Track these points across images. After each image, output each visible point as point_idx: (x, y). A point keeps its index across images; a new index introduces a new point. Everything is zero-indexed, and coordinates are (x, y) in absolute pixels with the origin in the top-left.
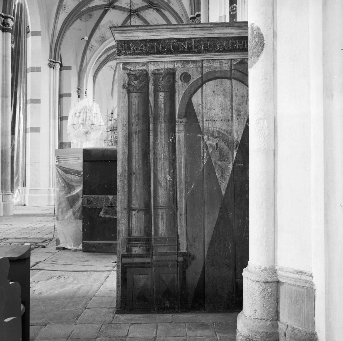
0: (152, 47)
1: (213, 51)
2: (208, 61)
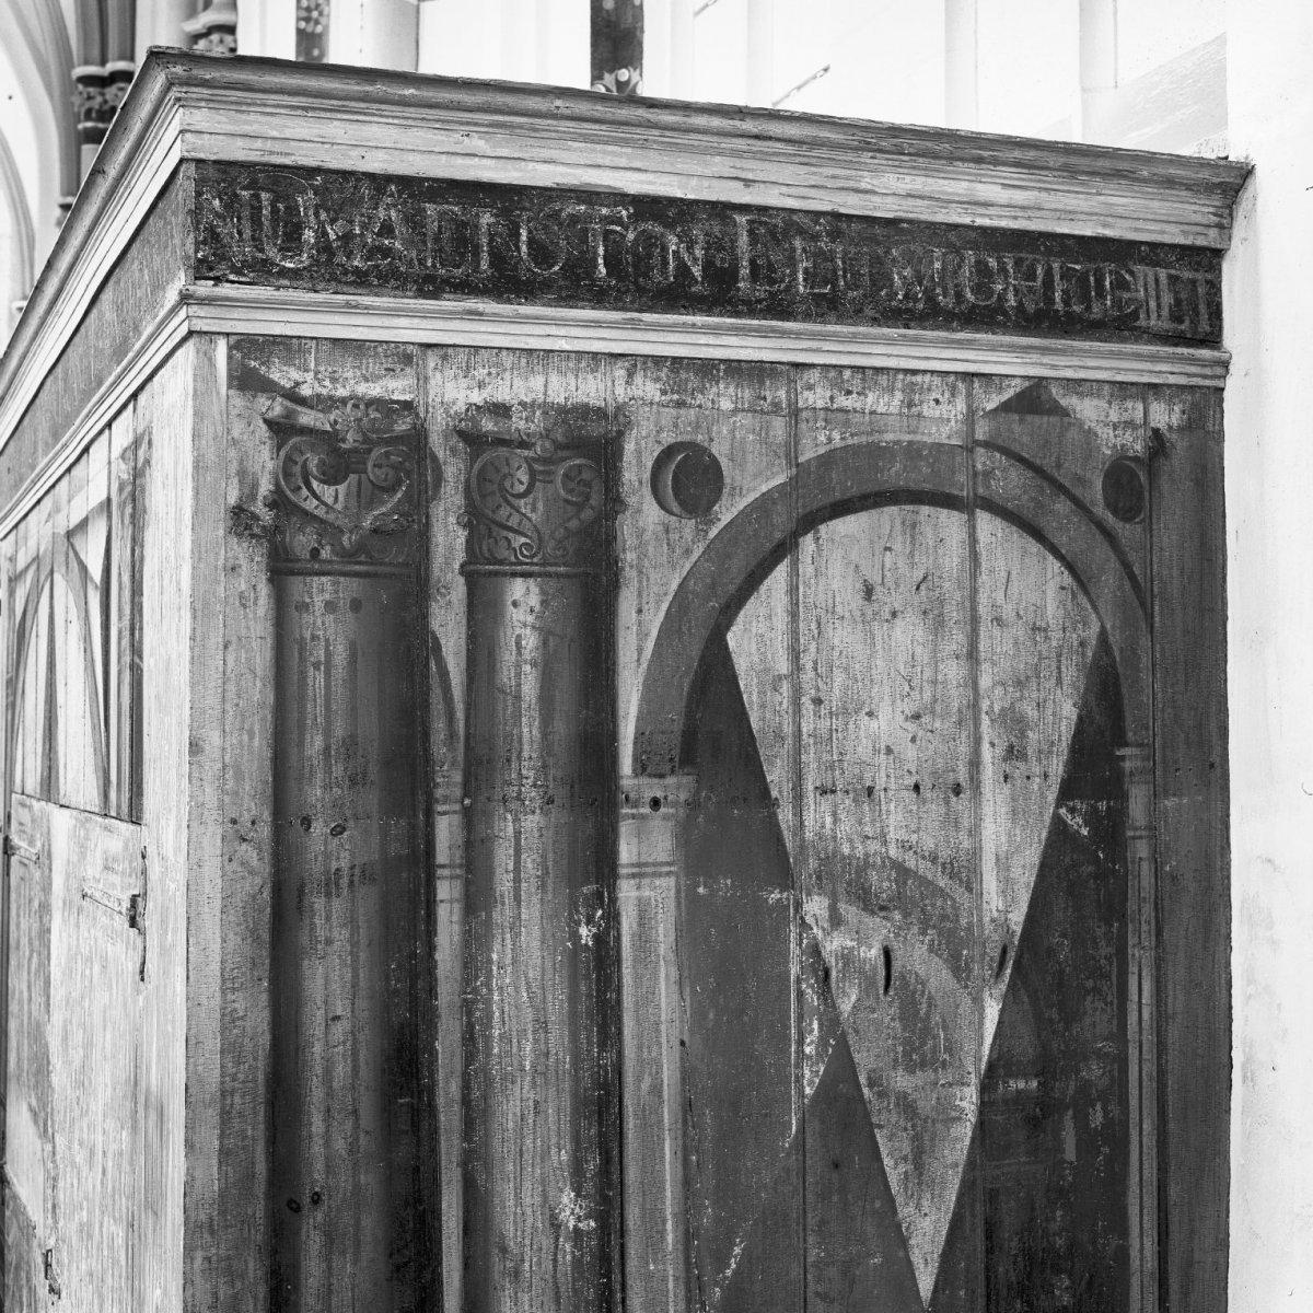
0: (462, 240)
1: (869, 312)
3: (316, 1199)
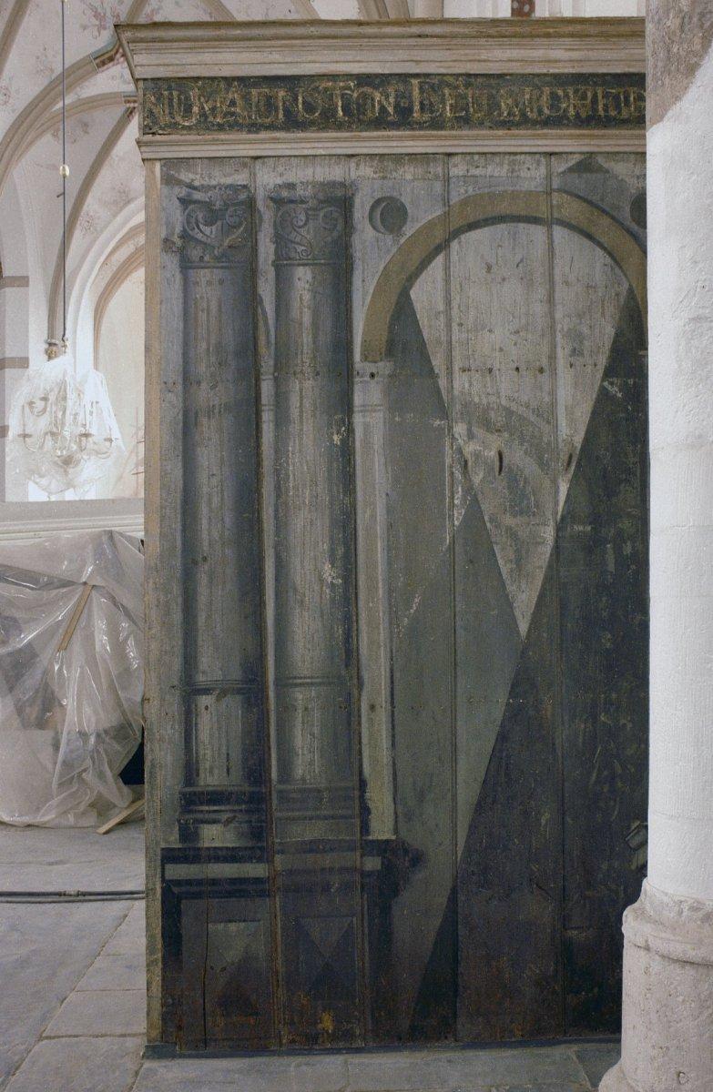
0: (270, 104)
2: (468, 157)
3: (205, 559)
